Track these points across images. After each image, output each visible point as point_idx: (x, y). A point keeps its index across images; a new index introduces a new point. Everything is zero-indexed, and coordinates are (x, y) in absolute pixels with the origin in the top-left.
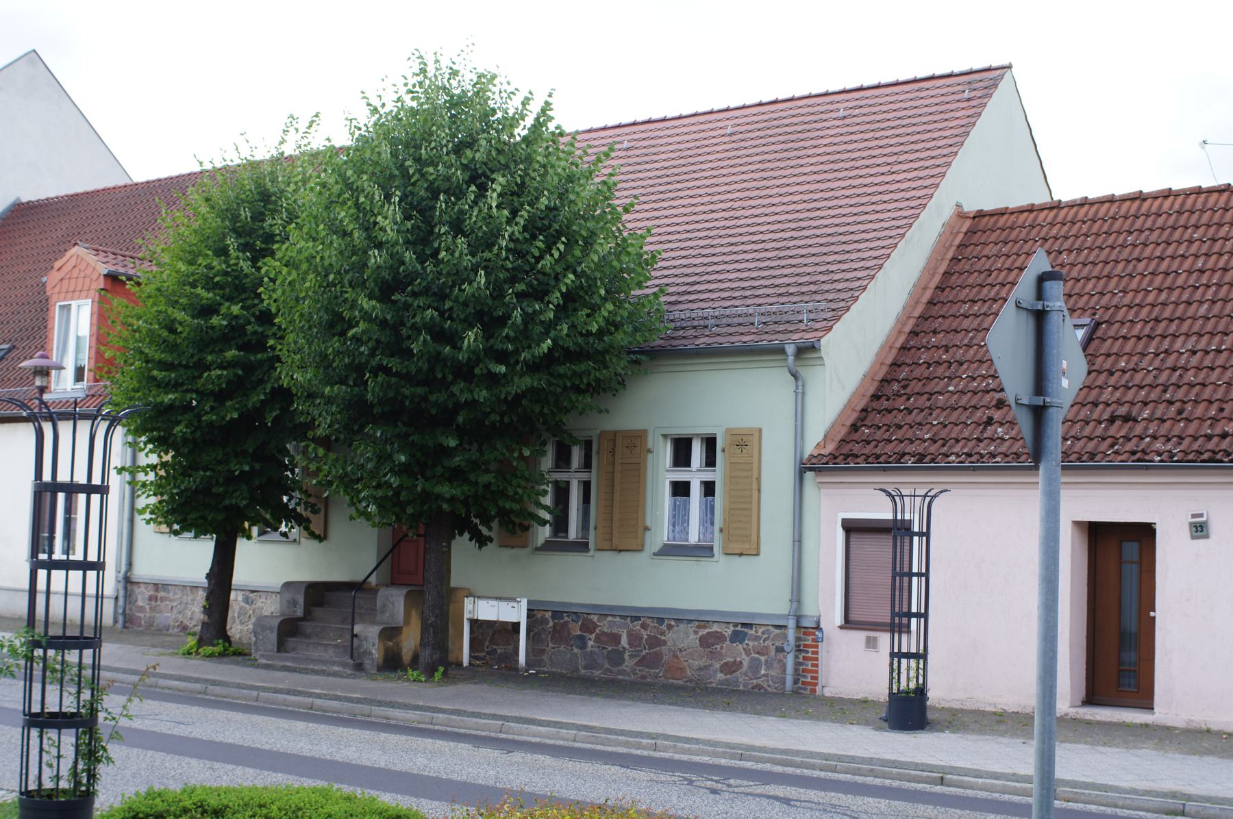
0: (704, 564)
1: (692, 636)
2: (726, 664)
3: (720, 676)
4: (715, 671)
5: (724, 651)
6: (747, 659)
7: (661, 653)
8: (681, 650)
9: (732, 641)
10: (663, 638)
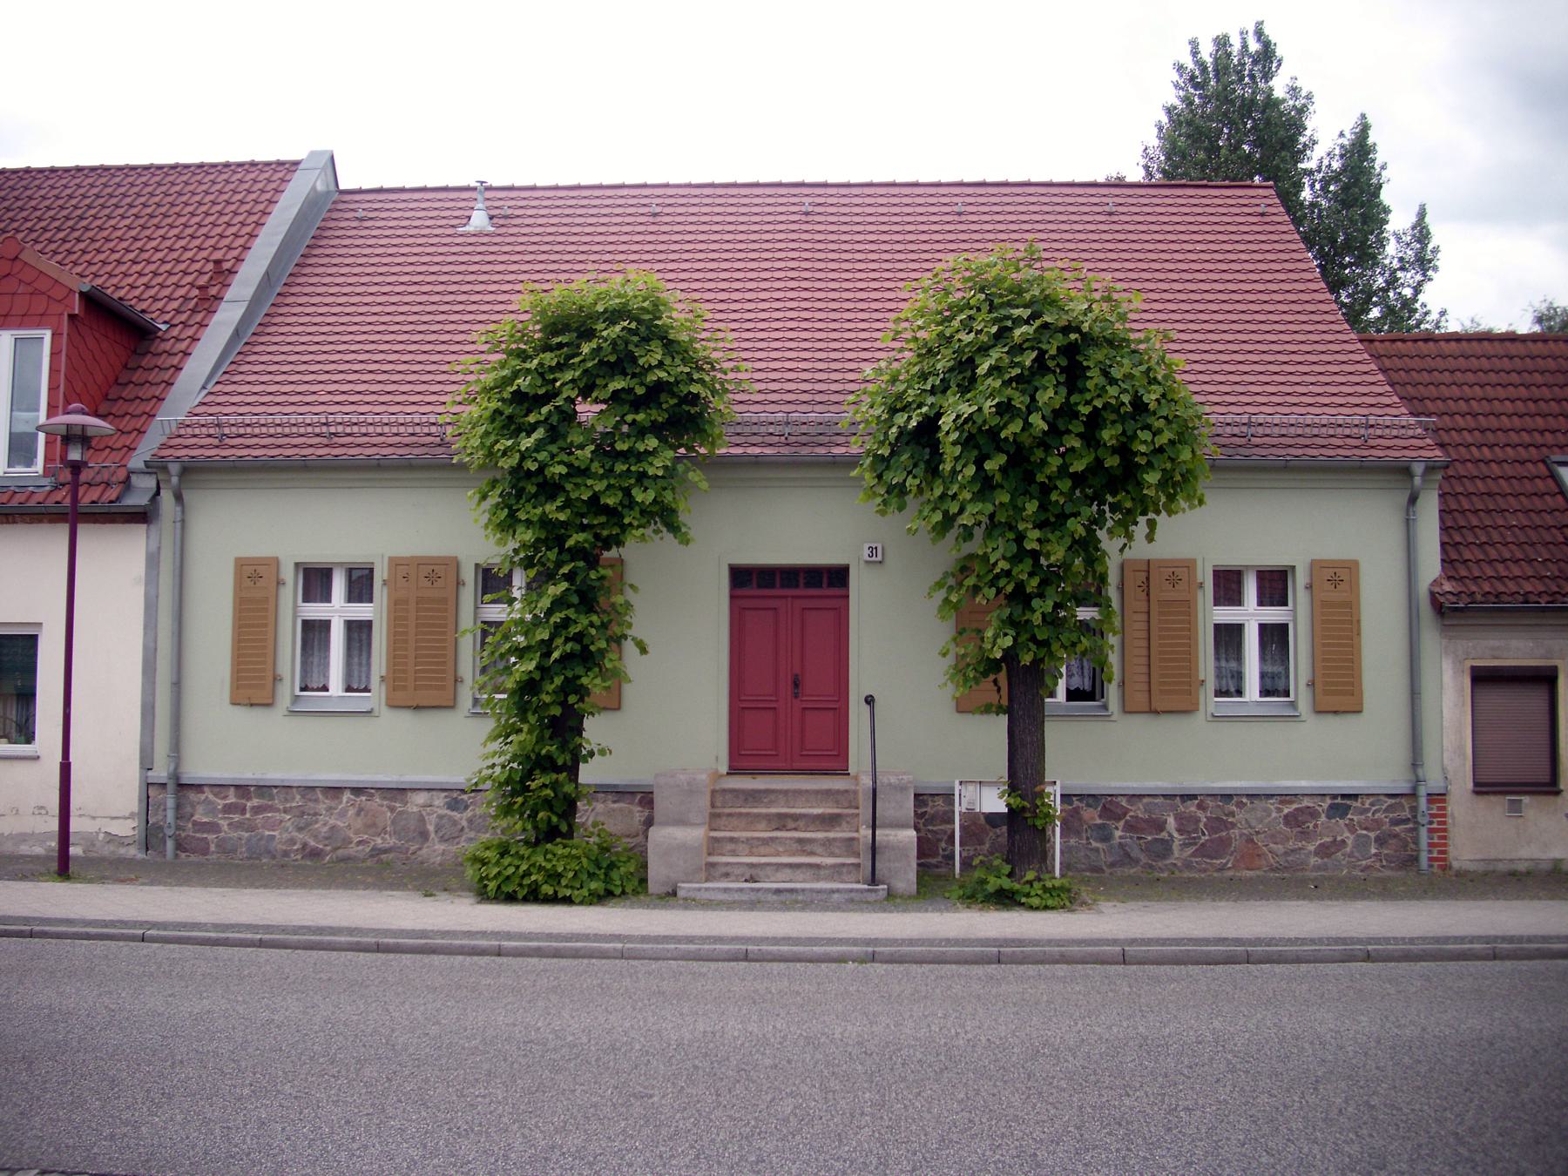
6: (1352, 837)
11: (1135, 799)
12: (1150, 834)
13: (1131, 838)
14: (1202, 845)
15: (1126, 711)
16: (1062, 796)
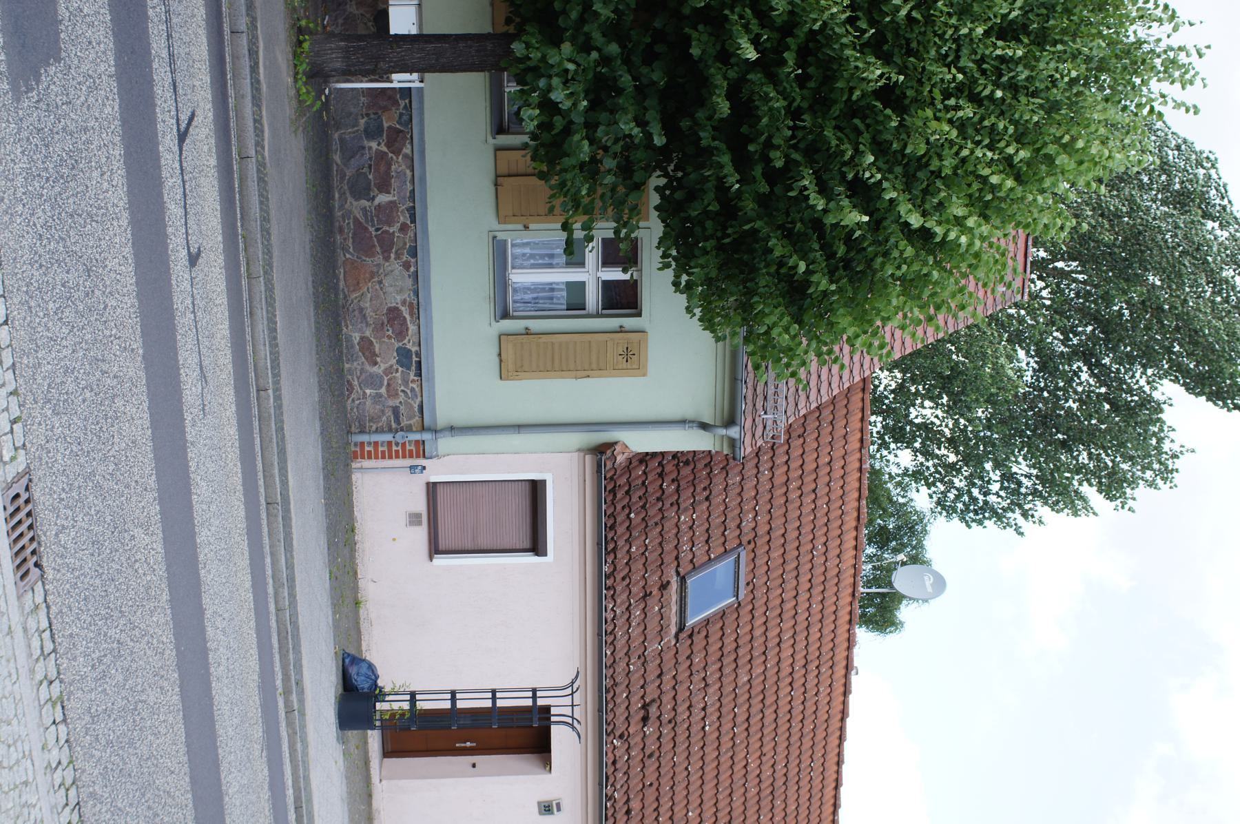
0: (485, 309)
1: (399, 298)
3: (356, 337)
4: (360, 330)
5: (386, 340)
7: (373, 255)
8: (380, 282)
10: (392, 256)
11: (409, 163)
12: (375, 178)
13: (370, 159)
14: (366, 229)
15: (498, 149)
16: (410, 89)
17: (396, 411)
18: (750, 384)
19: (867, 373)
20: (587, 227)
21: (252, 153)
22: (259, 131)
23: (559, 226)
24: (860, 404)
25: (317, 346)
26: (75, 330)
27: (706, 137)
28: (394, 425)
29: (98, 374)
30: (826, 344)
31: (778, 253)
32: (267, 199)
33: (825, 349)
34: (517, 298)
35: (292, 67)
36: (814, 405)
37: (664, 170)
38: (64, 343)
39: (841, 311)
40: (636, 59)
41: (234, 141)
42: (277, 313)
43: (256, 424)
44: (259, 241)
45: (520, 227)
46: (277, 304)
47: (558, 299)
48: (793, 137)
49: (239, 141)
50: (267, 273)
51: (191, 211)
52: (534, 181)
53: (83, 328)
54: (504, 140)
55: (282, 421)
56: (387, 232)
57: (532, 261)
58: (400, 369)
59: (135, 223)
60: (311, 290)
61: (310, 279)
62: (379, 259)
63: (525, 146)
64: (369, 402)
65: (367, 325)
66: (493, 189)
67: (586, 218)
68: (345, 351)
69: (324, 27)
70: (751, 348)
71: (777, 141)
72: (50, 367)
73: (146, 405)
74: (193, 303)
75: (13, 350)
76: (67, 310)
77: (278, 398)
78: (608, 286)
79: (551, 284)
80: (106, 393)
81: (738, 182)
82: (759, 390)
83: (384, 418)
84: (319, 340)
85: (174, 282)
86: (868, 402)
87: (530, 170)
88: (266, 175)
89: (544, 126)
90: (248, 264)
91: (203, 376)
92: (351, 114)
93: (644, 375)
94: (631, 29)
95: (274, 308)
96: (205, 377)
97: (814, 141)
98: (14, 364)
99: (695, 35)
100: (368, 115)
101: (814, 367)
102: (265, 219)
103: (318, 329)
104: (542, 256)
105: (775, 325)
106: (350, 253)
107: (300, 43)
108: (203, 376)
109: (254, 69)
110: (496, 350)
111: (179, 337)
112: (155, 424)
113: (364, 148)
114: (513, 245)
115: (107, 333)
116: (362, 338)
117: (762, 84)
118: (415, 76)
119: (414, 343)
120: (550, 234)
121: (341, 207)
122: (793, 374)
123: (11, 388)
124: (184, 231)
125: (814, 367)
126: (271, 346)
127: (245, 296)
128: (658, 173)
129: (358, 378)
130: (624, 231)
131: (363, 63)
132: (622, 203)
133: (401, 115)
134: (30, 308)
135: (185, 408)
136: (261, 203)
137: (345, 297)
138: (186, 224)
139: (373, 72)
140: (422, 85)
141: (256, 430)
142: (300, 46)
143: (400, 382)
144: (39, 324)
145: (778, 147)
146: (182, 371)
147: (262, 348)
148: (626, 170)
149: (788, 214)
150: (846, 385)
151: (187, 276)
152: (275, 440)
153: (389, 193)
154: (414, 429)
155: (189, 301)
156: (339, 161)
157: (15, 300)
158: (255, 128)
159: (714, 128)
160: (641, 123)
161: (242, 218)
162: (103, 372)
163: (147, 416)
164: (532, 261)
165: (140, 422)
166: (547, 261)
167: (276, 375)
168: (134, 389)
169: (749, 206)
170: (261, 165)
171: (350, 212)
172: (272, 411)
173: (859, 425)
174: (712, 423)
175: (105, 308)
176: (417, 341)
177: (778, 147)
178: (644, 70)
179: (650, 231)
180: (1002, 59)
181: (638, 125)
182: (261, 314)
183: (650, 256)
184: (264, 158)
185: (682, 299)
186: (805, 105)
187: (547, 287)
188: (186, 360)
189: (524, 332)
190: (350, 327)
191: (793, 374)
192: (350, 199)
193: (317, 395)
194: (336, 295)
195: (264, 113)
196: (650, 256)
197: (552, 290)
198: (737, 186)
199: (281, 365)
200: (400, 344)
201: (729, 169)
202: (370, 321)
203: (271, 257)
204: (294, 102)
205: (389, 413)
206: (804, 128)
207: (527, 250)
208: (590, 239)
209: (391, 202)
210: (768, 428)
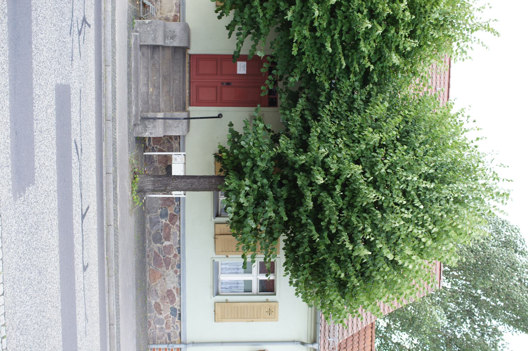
0: (209, 291)
1: (172, 286)
2: (159, 305)
3: (153, 302)
4: (155, 299)
5: (166, 304)
7: (161, 267)
8: (164, 279)
9: (171, 308)
10: (170, 268)
11: (178, 228)
12: (164, 235)
13: (162, 226)
14: (159, 256)
15: (216, 223)
16: (180, 198)
17: (169, 335)
18: (323, 325)
19: (373, 321)
20: (253, 257)
21: (112, 223)
22: (116, 214)
23: (241, 256)
24: (371, 334)
25: (136, 306)
26: (32, 298)
27: (304, 220)
28: (168, 341)
29: (41, 317)
30: (355, 308)
31: (333, 269)
32: (118, 243)
33: (354, 311)
34: (223, 286)
35: (131, 188)
36: (350, 335)
37: (286, 233)
38: (27, 304)
39: (361, 294)
40: (275, 186)
41: (105, 218)
42: (120, 291)
43: (108, 340)
44: (113, 261)
45: (225, 256)
46: (120, 288)
47: (240, 287)
48: (339, 220)
49: (107, 218)
50: (116, 274)
51: (85, 248)
52: (231, 237)
53: (36, 297)
54: (219, 219)
55: (119, 339)
56: (168, 257)
57: (229, 271)
58: (172, 317)
59: (61, 253)
60: (135, 282)
61: (135, 277)
62: (164, 269)
63: (227, 222)
64: (157, 331)
65: (158, 297)
66: (213, 240)
67: (253, 252)
68: (148, 308)
69: (145, 172)
70: (324, 310)
71: (332, 222)
72: (20, 314)
73: (61, 331)
74: (84, 287)
75: (5, 306)
76: (30, 290)
77: (118, 328)
78: (262, 282)
79: (237, 281)
80: (44, 326)
81: (318, 237)
82: (327, 328)
83: (164, 338)
84: (137, 304)
85: (76, 278)
86: (374, 333)
87: (229, 233)
88: (118, 233)
89: (236, 213)
90: (108, 270)
91: (86, 319)
92: (154, 208)
93: (277, 321)
94: (273, 175)
95: (118, 289)
96: (87, 319)
97: (348, 221)
98: (5, 313)
99: (299, 176)
100: (162, 208)
101: (350, 318)
102: (117, 251)
103: (137, 299)
104: (234, 269)
105: (334, 299)
106: (152, 266)
107: (135, 178)
108: (86, 319)
109: (115, 188)
110: (214, 309)
111: (77, 302)
112: (64, 340)
113: (159, 222)
114: (221, 264)
115: (46, 299)
116: (156, 303)
117: (326, 198)
118: (182, 192)
119: (178, 305)
120: (237, 260)
121: (149, 246)
122: (341, 322)
123: (3, 323)
124: (82, 256)
125: (350, 318)
126: (116, 306)
127: (106, 284)
128: (283, 234)
129: (153, 320)
130: (268, 258)
131: (160, 187)
132: (268, 247)
133: (176, 208)
134: (14, 288)
135: (77, 333)
136: (115, 244)
137: (149, 285)
138: (83, 253)
139: (165, 190)
140: (185, 196)
141: (108, 343)
142: (135, 180)
143: (171, 322)
144: (17, 295)
145: (333, 224)
146: (77, 316)
147: (112, 306)
148: (270, 232)
149: (338, 252)
150: (365, 326)
151: (82, 275)
152: (116, 347)
153: (169, 241)
154: (177, 343)
155: (82, 286)
156: (149, 227)
157: (7, 285)
158: (114, 213)
159: (307, 216)
160: (276, 212)
161: (107, 251)
162: (43, 317)
163: (61, 336)
164: (229, 271)
165: (58, 338)
166: (236, 271)
167: (118, 318)
168: (56, 324)
169: (322, 248)
170: (116, 229)
171: (153, 249)
172: (115, 334)
173: (370, 343)
174: (306, 342)
175: (46, 289)
176: (179, 304)
177: (333, 224)
178: (278, 190)
179: (280, 259)
180: (426, 189)
181: (274, 213)
182: (113, 292)
183: (280, 269)
184: (117, 226)
185: (293, 289)
186: (344, 207)
187: (236, 282)
188: (79, 312)
189: (225, 301)
190: (151, 298)
191: (341, 322)
192: (153, 243)
193: (135, 327)
194: (145, 284)
195: (118, 207)
196: (280, 269)
197: (238, 283)
198: (318, 239)
199: (120, 314)
200: (172, 306)
201: (314, 232)
202: (160, 295)
203: (118, 268)
204: (131, 202)
205: (166, 336)
206: (344, 216)
207: (228, 266)
208: (254, 262)
209: (170, 245)
210: (330, 345)
